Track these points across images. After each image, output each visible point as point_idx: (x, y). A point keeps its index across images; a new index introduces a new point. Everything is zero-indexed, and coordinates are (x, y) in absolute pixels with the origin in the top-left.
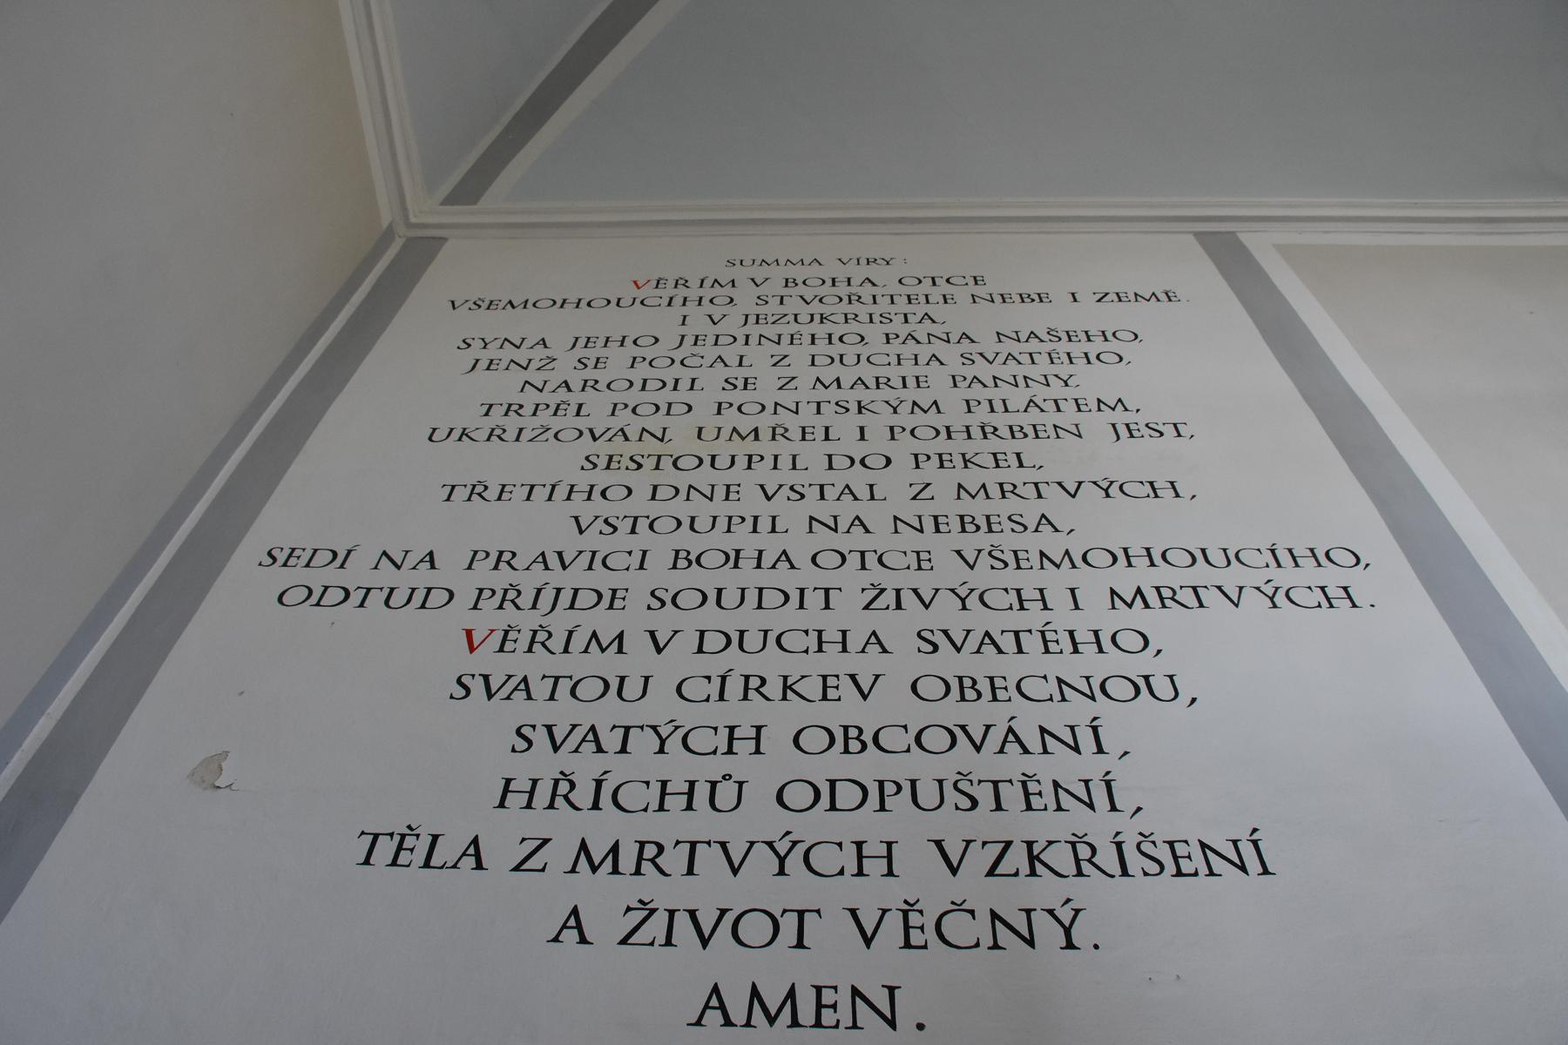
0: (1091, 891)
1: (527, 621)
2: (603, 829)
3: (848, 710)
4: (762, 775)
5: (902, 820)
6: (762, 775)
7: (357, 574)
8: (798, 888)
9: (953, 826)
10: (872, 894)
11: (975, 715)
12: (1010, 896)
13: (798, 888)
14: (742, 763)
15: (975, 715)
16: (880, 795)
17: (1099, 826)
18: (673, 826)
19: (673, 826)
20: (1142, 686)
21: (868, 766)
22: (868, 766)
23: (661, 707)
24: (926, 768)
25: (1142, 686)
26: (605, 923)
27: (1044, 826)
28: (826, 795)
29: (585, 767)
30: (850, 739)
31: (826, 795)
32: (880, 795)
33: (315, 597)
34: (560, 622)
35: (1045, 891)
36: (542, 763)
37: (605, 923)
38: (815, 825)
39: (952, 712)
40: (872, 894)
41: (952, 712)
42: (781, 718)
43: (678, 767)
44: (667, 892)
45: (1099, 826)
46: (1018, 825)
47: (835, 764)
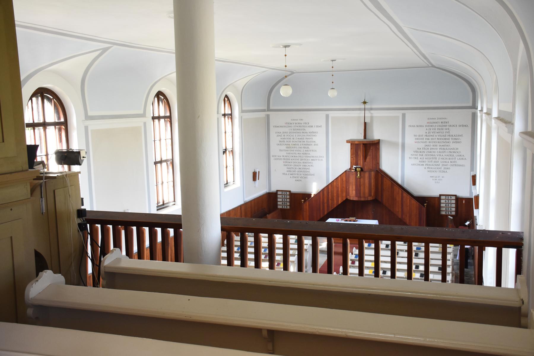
0: (308, 176)
1: (286, 161)
2: (291, 173)
3: (300, 167)
4: (297, 170)
5: (301, 173)
6: (297, 170)
7: (277, 157)
8: (298, 176)
9: (303, 173)
10: (300, 176)
11: (305, 167)
12: (305, 176)
13: (298, 176)
14: (296, 170)
15: (305, 167)
16: (301, 171)
17: (309, 173)
18: (293, 173)
19: (293, 173)
20: (312, 166)
21: (300, 170)
22: (300, 170)
23: (292, 167)
24: (303, 170)
25: (312, 166)
26: (292, 177)
27: (307, 173)
28: (299, 171)
29: (290, 170)
30: (300, 169)
31: (299, 171)
32: (301, 171)
33: (276, 159)
34: (287, 161)
35: (306, 176)
36: (288, 170)
37: (292, 177)
38: (299, 173)
39: (304, 167)
40: (300, 176)
41: (304, 167)
42: (297, 167)
43: (293, 170)
44: (294, 176)
45: (309, 173)
46: (306, 173)
47: (299, 170)
